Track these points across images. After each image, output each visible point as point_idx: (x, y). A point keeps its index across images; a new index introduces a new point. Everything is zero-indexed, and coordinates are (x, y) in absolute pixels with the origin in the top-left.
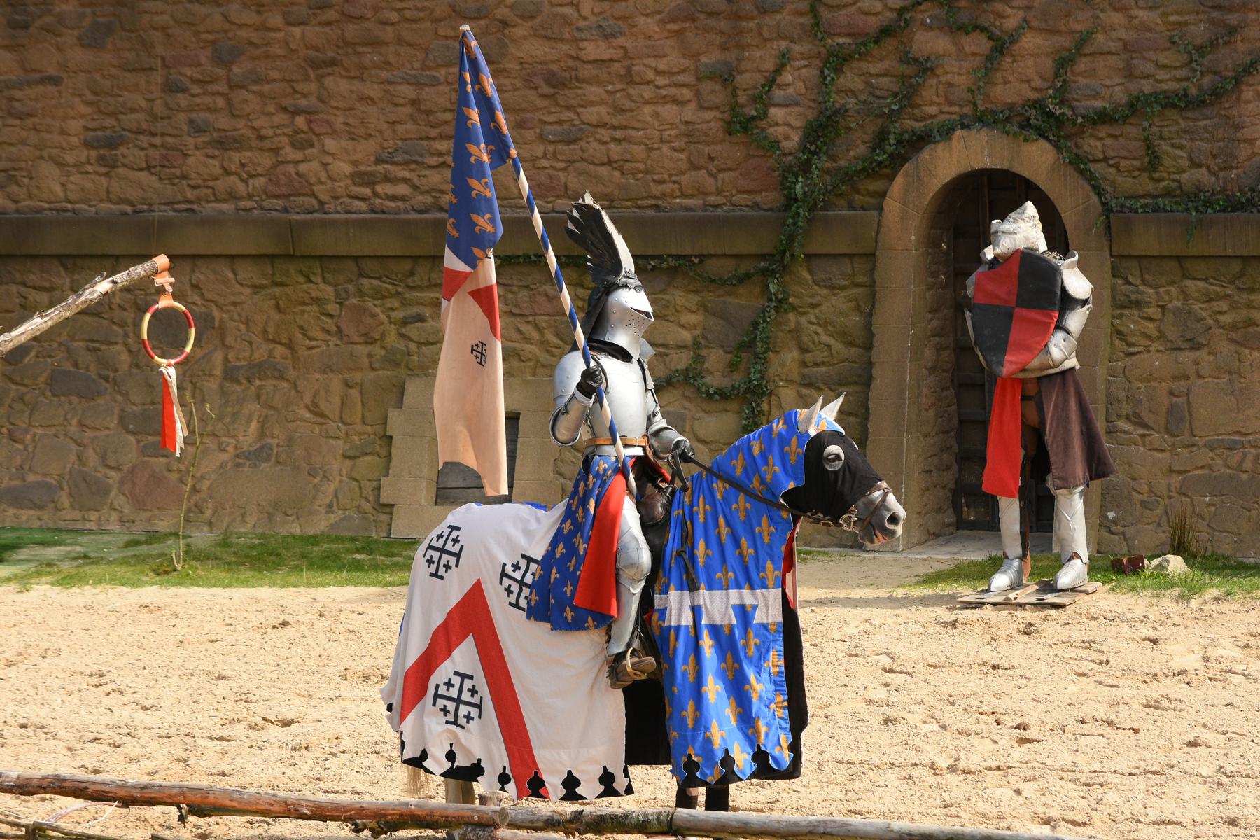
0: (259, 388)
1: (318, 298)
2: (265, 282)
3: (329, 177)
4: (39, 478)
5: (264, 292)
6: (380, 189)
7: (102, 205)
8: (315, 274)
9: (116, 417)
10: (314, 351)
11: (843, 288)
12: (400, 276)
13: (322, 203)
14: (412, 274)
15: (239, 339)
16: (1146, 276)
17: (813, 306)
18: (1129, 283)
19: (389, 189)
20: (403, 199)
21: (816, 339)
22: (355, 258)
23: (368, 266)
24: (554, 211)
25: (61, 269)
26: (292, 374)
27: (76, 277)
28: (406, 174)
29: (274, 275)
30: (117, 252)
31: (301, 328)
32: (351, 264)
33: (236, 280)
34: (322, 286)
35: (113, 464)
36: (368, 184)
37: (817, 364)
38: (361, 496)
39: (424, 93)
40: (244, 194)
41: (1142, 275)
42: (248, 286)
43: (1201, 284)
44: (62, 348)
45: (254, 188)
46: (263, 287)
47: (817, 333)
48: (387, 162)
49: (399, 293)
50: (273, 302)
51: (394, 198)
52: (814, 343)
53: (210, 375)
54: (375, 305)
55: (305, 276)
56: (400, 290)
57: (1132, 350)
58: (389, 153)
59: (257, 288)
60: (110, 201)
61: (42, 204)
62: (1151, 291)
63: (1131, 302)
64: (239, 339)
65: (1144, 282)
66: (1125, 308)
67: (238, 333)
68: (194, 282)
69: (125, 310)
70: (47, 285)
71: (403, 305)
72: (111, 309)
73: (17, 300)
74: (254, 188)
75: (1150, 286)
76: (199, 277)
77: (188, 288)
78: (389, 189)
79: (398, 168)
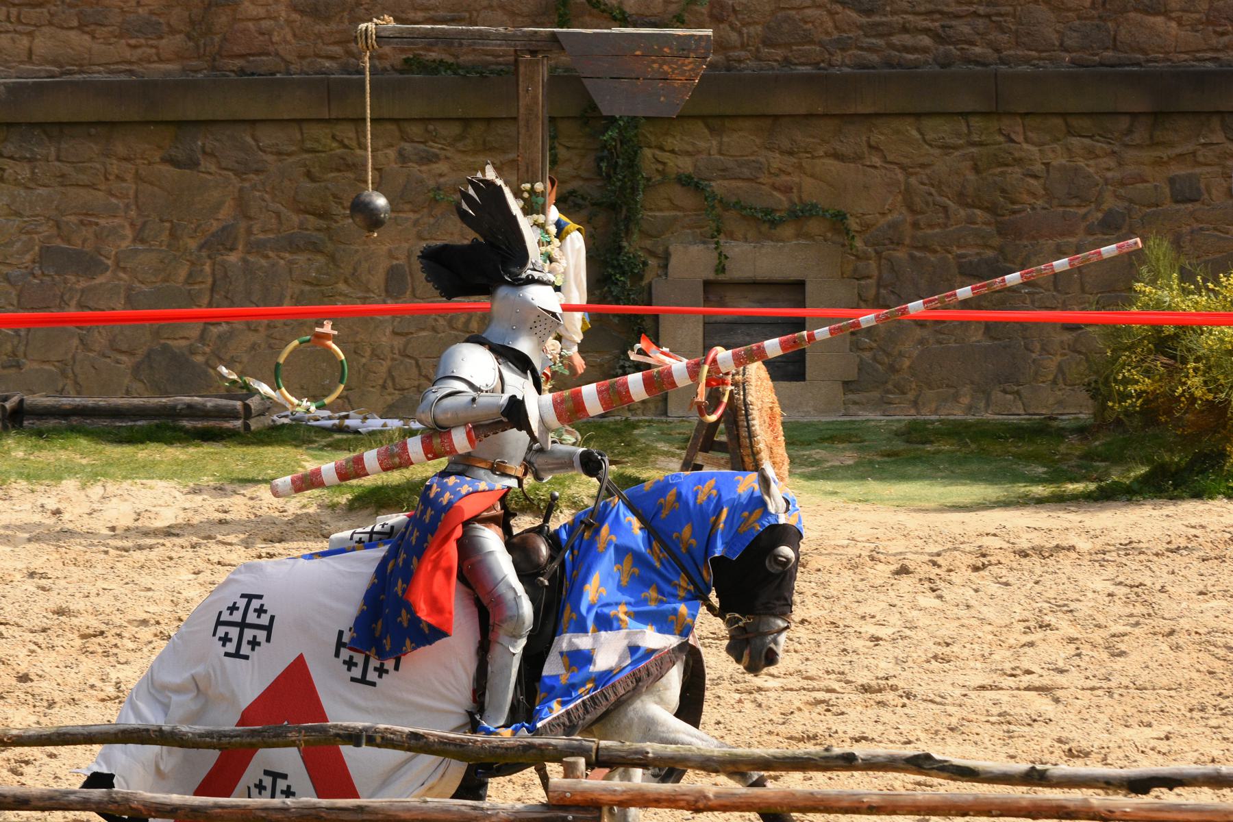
0: (291, 262)
1: (1021, 159)
2: (294, 148)
3: (836, 28)
4: (36, 366)
5: (957, 153)
6: (895, 40)
7: (1105, 54)
9: (122, 295)
10: (1018, 216)
11: (956, 148)
12: (1116, 134)
13: (288, 63)
14: (1130, 131)
15: (264, 210)
16: (1029, 134)
17: (923, 166)
18: (1012, 141)
19: (907, 39)
20: (925, 50)
21: (930, 199)
22: (1064, 115)
23: (1076, 123)
24: (1102, 64)
25: (44, 137)
26: (330, 247)
27: (64, 146)
28: (928, 24)
29: (970, 133)
30: (252, 117)
31: (335, 196)
32: (1058, 121)
33: (925, 141)
34: (1025, 146)
35: (124, 347)
36: (881, 36)
37: (931, 226)
38: (420, 374)
40: (738, 44)
41: (1025, 132)
42: (271, 153)
43: (1087, 141)
44: (51, 223)
45: (749, 36)
46: (956, 148)
47: (931, 194)
48: (906, 12)
49: (1114, 152)
50: (969, 163)
51: (914, 50)
52: (927, 204)
53: (898, 244)
54: (1087, 165)
55: (1004, 135)
56: (1116, 149)
57: (1017, 207)
58: (366, 9)
59: (947, 148)
60: (1115, 48)
61: (1030, 53)
62: (1034, 149)
63: (1014, 159)
64: (264, 210)
65: (1027, 140)
67: (263, 204)
68: (873, 143)
69: (123, 180)
70: (690, 148)
71: (1120, 165)
72: (107, 179)
73: (654, 166)
74: (749, 36)
75: (1034, 144)
76: (876, 138)
77: (866, 150)
78: (907, 39)
79: (918, 18)
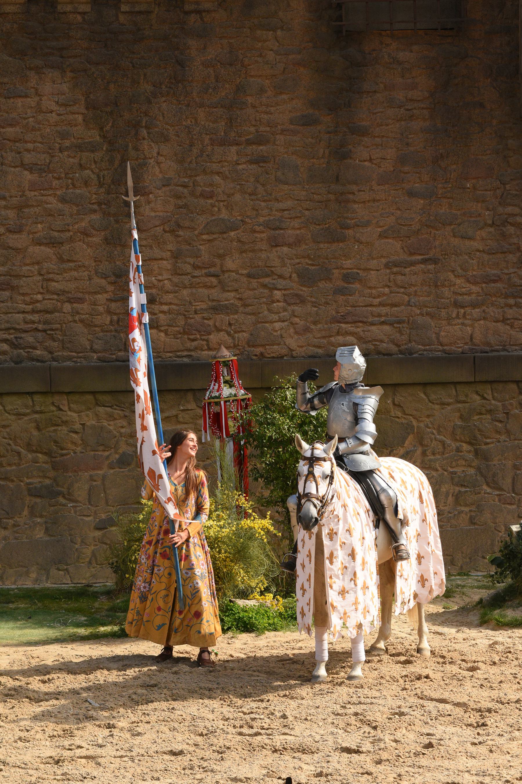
1: (66, 422)
5: (26, 418)
8: (64, 405)
10: (65, 457)
11: (25, 415)
16: (72, 405)
18: (61, 410)
21: (9, 448)
22: (93, 393)
23: (100, 397)
24: (117, 360)
29: (34, 405)
32: (90, 397)
33: (5, 410)
34: (69, 413)
37: (10, 465)
39: (22, 282)
41: (69, 405)
46: (25, 415)
47: (9, 445)
50: (33, 425)
54: (109, 425)
55: (55, 406)
56: (127, 414)
57: (64, 452)
59: (19, 415)
62: (75, 415)
63: (62, 422)
66: (58, 425)
71: (129, 424)
75: (75, 411)
